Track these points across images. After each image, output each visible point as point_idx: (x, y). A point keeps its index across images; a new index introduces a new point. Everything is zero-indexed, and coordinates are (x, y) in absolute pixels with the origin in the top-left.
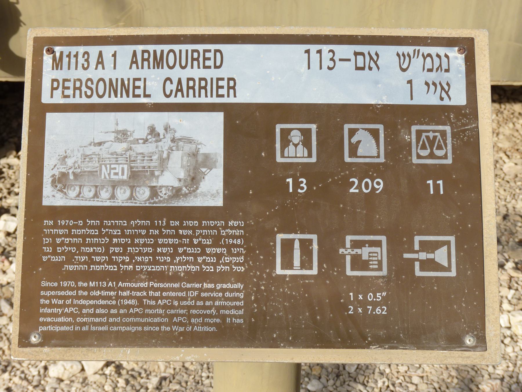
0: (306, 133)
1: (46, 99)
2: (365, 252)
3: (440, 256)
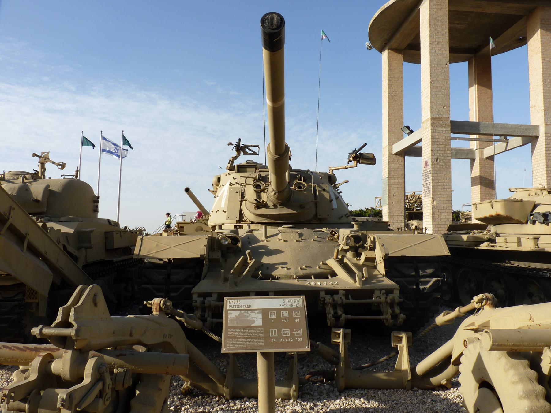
0: (274, 313)
1: (228, 308)
2: (286, 332)
3: (299, 332)
